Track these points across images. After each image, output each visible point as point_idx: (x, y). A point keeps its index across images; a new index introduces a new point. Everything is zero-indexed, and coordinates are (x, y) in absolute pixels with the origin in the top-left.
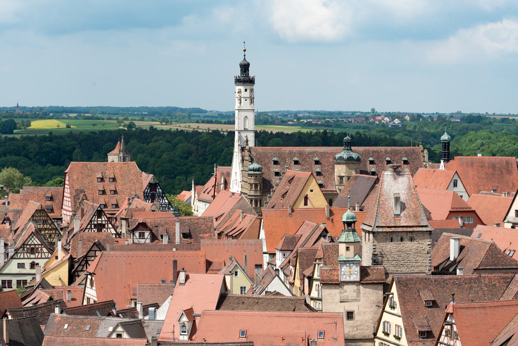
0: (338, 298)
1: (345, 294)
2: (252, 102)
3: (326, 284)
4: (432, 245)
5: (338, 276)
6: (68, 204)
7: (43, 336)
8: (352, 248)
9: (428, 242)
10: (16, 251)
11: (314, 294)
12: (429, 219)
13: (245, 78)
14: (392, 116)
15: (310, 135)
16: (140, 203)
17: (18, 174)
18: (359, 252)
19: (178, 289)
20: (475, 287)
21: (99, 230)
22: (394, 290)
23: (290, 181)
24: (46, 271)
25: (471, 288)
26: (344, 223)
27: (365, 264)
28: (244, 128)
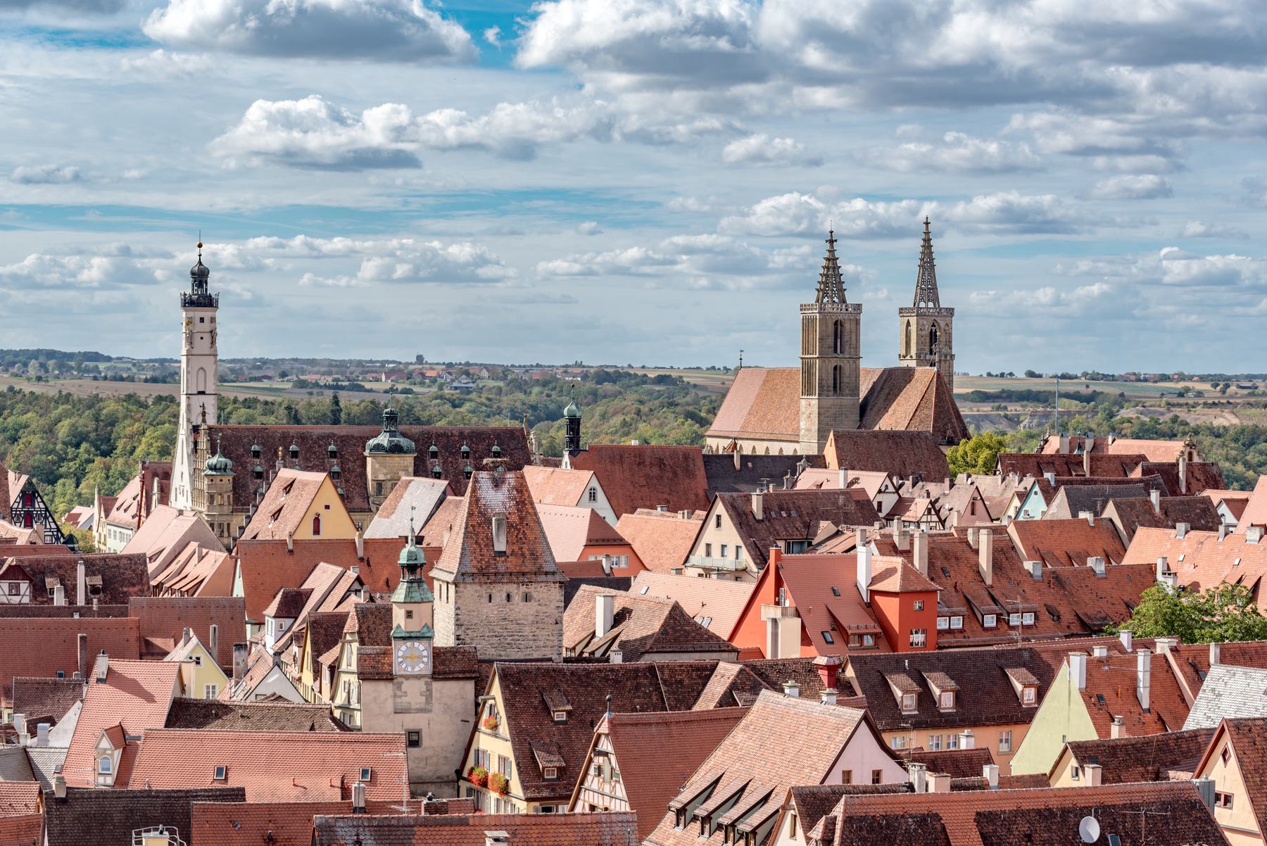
0: (389, 707)
1: (404, 699)
5: (391, 665)
20: (645, 686)
23: (288, 488)
25: (637, 687)
26: (403, 566)
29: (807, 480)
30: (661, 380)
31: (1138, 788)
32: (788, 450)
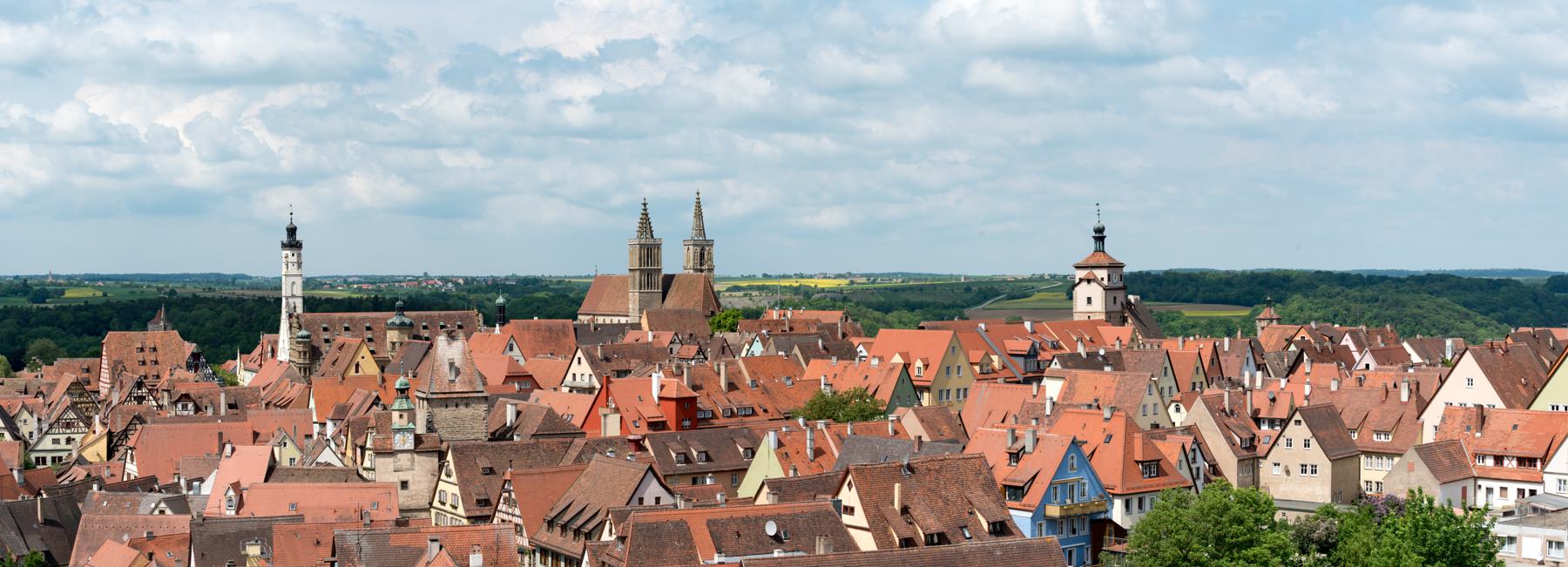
0: (391, 468)
2: (300, 265)
3: (379, 453)
4: (489, 411)
6: (105, 376)
7: (80, 514)
8: (405, 415)
9: (484, 407)
10: (51, 426)
11: (367, 464)
12: (485, 384)
13: (293, 243)
14: (445, 280)
15: (360, 300)
16: (182, 373)
17: (52, 345)
18: (412, 419)
19: (224, 463)
21: (140, 403)
22: (450, 457)
23: (340, 348)
24: (83, 448)
27: (419, 432)
28: (292, 293)
29: (630, 337)
30: (559, 282)
31: (802, 506)
32: (623, 320)
